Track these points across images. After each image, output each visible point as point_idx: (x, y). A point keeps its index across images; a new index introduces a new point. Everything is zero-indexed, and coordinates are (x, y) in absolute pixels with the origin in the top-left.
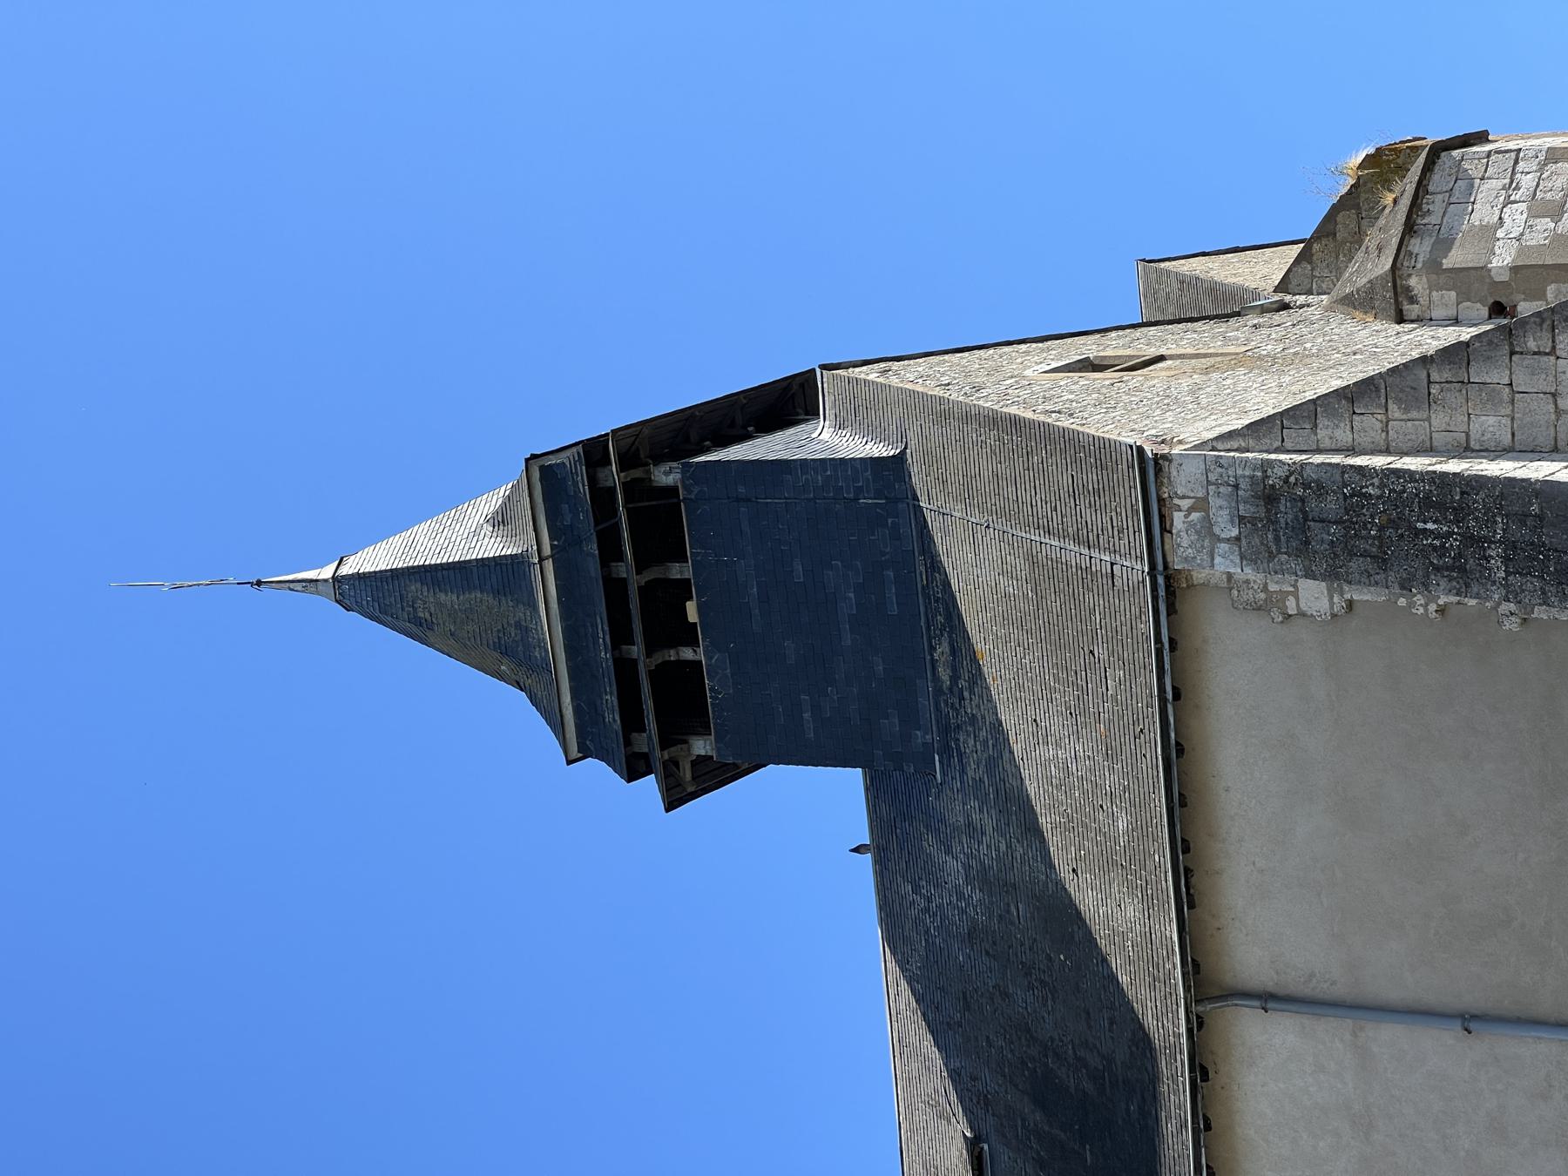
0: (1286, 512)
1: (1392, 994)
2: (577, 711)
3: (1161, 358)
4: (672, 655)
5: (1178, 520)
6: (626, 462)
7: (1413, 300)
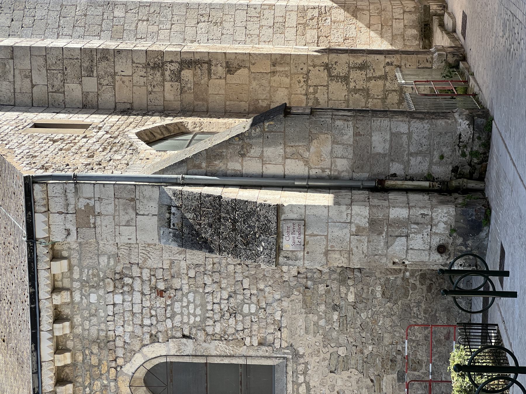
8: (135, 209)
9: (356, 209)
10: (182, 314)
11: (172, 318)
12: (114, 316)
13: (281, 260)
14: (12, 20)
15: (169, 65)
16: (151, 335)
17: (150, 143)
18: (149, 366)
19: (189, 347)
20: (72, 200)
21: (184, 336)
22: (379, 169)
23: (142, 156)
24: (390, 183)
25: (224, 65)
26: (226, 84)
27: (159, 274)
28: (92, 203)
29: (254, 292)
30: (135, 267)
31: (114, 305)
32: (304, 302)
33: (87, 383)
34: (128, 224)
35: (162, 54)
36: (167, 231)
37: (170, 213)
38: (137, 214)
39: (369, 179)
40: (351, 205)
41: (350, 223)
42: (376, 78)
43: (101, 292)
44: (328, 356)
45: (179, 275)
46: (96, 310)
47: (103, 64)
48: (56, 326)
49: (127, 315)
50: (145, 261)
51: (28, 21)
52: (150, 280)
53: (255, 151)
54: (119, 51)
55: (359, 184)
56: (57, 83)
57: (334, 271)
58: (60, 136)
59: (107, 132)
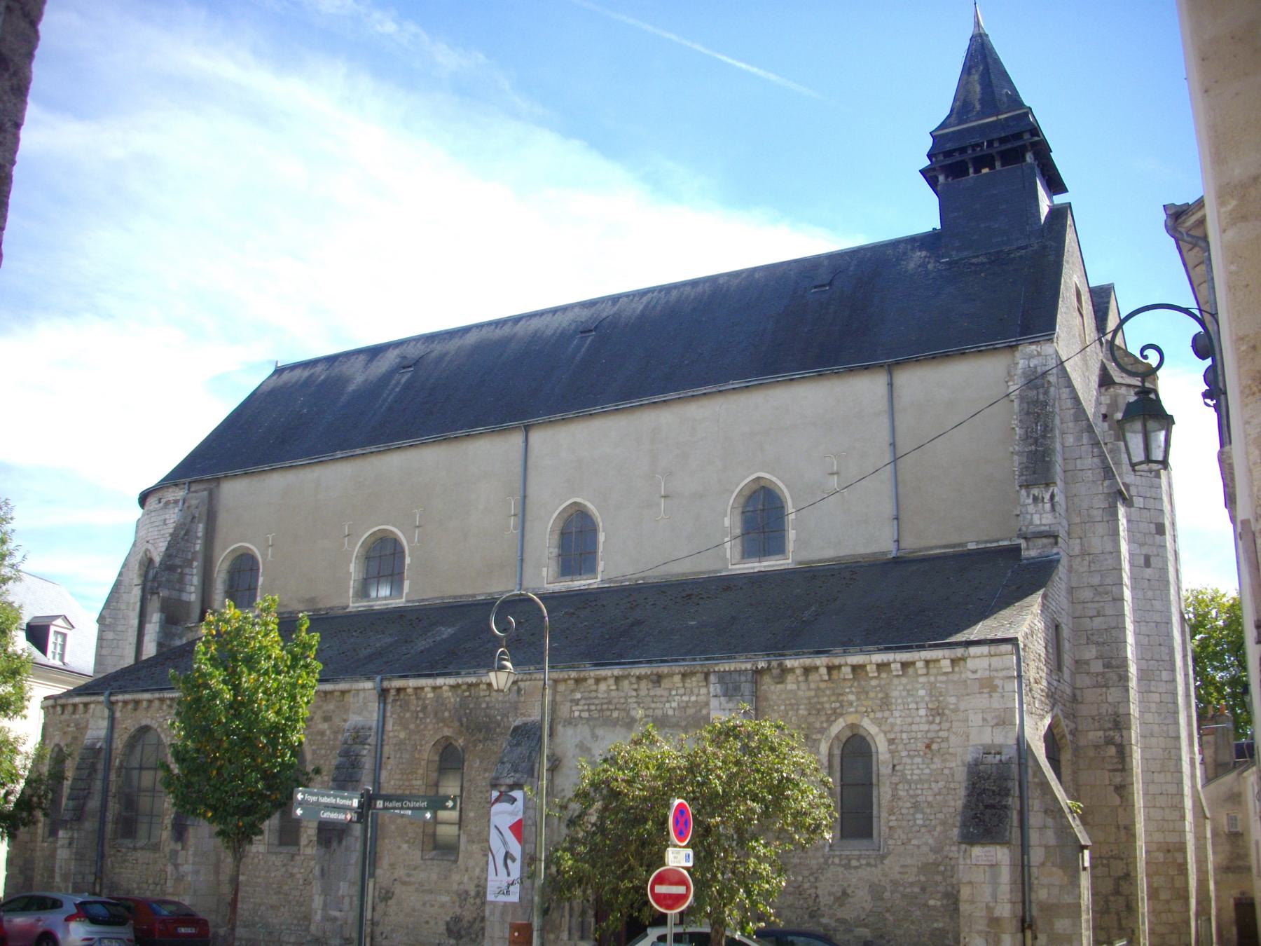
1: (897, 423)
2: (947, 134)
4: (970, 165)
5: (1033, 347)
6: (1033, 144)
7: (1106, 390)
8: (997, 724)
9: (1008, 907)
10: (912, 764)
11: (909, 756)
12: (908, 709)
14: (1149, 580)
15: (1119, 735)
16: (893, 739)
18: (868, 738)
19: (885, 770)
20: (1001, 674)
22: (1040, 923)
23: (1039, 724)
24: (1029, 934)
25: (1123, 783)
26: (1105, 786)
27: (944, 745)
28: (1000, 690)
29: (933, 823)
30: (948, 725)
31: (917, 709)
32: (928, 864)
33: (853, 689)
34: (984, 720)
35: (1129, 728)
36: (981, 751)
37: (995, 754)
38: (992, 727)
39: (1031, 918)
40: (1011, 902)
41: (996, 902)
42: (1119, 920)
43: (927, 699)
44: (883, 883)
45: (944, 761)
46: (912, 695)
47: (1115, 678)
48: (899, 665)
49: (910, 720)
50: (955, 734)
51: (1150, 593)
52: (939, 737)
54: (1127, 691)
55: (1027, 908)
56: (1095, 638)
57: (953, 888)
59: (1056, 688)
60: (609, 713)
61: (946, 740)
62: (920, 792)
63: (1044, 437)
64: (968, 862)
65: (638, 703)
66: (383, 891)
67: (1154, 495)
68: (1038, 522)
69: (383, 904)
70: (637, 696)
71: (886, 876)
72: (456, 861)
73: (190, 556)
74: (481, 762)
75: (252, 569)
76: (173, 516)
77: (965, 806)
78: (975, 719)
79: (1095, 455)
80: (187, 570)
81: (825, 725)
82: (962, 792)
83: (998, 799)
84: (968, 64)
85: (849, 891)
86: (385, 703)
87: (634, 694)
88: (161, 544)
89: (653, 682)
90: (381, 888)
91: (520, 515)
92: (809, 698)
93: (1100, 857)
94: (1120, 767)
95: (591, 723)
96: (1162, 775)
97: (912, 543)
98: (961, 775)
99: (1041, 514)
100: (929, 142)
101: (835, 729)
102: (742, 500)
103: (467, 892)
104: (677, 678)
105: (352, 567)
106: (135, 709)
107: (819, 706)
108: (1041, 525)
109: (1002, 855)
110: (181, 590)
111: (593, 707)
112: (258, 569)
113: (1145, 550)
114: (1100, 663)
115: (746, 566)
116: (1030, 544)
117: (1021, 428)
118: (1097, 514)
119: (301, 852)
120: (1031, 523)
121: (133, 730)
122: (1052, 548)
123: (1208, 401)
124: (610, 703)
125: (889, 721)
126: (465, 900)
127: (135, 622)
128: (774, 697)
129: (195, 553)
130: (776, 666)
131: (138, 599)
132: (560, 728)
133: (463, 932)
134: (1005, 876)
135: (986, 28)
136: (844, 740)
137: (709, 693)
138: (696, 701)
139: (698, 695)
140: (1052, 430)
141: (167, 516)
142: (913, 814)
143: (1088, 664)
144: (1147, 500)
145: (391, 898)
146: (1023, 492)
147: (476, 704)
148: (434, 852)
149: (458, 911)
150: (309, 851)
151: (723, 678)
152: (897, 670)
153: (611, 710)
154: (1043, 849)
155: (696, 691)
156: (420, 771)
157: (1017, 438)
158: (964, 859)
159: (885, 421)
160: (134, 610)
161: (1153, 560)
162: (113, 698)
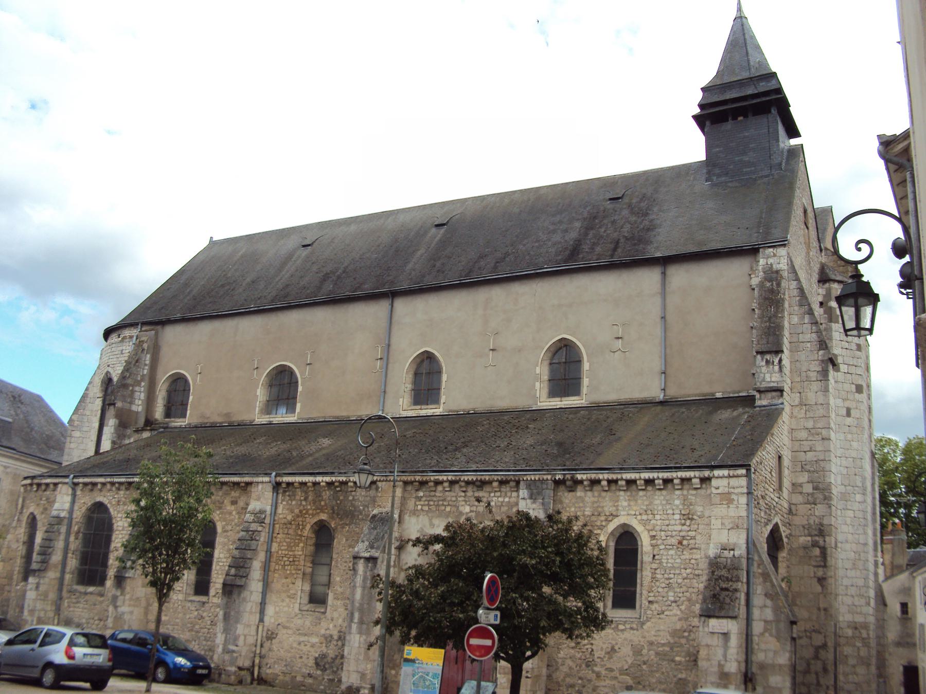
0: (774, 275)
3: (808, 228)
5: (771, 250)
8: (732, 528)
10: (668, 555)
13: (703, 619)
17: (772, 531)
18: (636, 535)
19: (647, 558)
20: (736, 491)
21: (654, 556)
27: (692, 542)
28: (735, 503)
30: (696, 526)
31: (673, 514)
34: (722, 524)
36: (720, 547)
43: (681, 507)
47: (821, 496)
48: (661, 481)
49: (667, 522)
51: (849, 436)
53: (769, 602)
56: (808, 467)
58: (774, 475)
60: (443, 508)
61: (694, 538)
62: (672, 576)
63: (775, 316)
64: (706, 629)
65: (465, 501)
66: (270, 633)
67: (855, 364)
68: (769, 380)
69: (270, 641)
70: (465, 496)
71: (645, 638)
72: (324, 613)
73: (139, 379)
74: (347, 540)
75: (184, 390)
76: (128, 348)
77: (706, 587)
78: (716, 523)
79: (813, 331)
80: (137, 388)
81: (604, 523)
82: (704, 578)
83: (730, 583)
84: (731, 39)
85: (616, 648)
86: (278, 494)
87: (463, 494)
88: (118, 368)
89: (478, 487)
90: (268, 630)
91: (385, 359)
92: (594, 502)
93: (805, 631)
94: (822, 564)
95: (430, 515)
96: (853, 571)
97: (674, 392)
98: (704, 565)
99: (771, 374)
100: (700, 95)
101: (612, 527)
102: (550, 355)
103: (331, 636)
104: (495, 484)
105: (259, 392)
106: (92, 490)
107: (600, 509)
108: (771, 382)
109: (733, 627)
110: (131, 403)
111: (432, 503)
112: (190, 390)
113: (847, 404)
114: (810, 485)
115: (551, 403)
116: (763, 395)
117: (759, 309)
118: (813, 375)
119: (210, 601)
120: (764, 380)
121: (89, 504)
122: (779, 399)
123: (902, 290)
124: (444, 500)
125: (652, 522)
126: (330, 641)
127: (96, 425)
128: (567, 501)
129: (143, 375)
130: (569, 477)
131: (99, 408)
132: (406, 517)
133: (327, 666)
134: (734, 641)
135: (746, 12)
136: (618, 535)
137: (518, 496)
138: (509, 502)
139: (510, 497)
140: (783, 311)
141: (124, 348)
142: (667, 592)
143: (802, 487)
144: (850, 367)
145: (275, 638)
146: (759, 357)
147: (345, 497)
148: (309, 606)
149: (325, 650)
150: (215, 600)
151: (530, 485)
152: (659, 485)
153: (445, 506)
154: (763, 623)
155: (509, 494)
156: (301, 545)
157: (756, 316)
158: (703, 627)
159: (658, 300)
160: (96, 416)
161: (852, 412)
162: (76, 480)
